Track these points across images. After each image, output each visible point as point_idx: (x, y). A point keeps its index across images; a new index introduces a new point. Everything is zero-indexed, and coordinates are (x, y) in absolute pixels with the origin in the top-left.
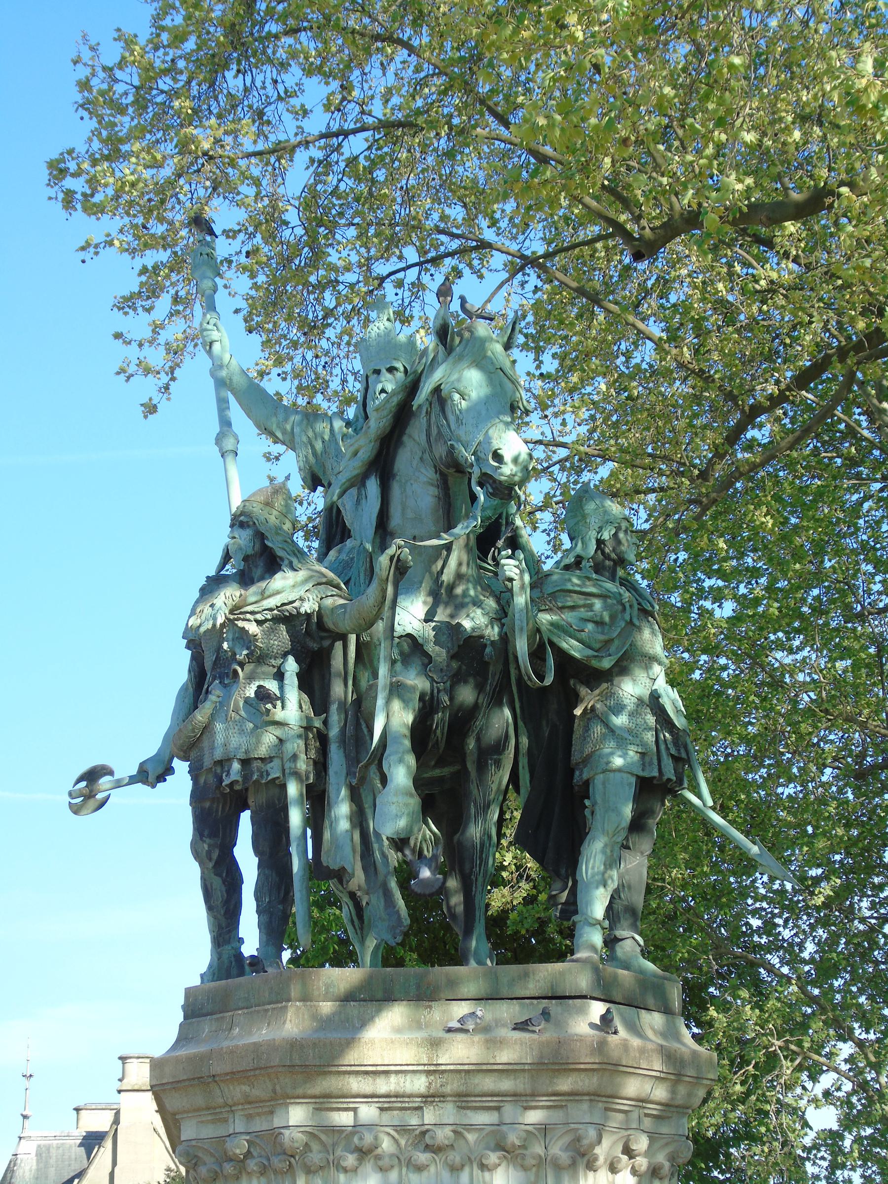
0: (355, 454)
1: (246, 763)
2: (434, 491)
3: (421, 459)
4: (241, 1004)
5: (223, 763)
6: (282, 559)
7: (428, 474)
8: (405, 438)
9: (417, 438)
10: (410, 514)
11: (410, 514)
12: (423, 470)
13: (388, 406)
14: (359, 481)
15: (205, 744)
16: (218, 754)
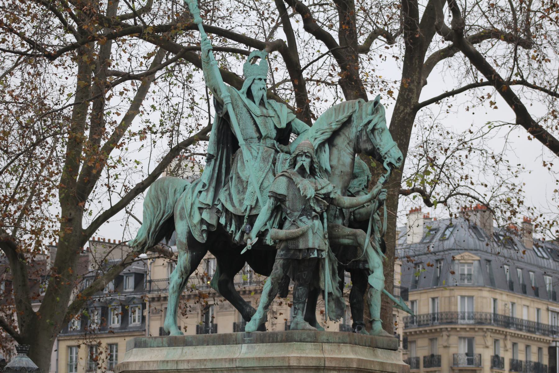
0: (322, 133)
1: (318, 250)
2: (351, 156)
3: (348, 144)
4: (324, 341)
5: (310, 250)
6: (316, 172)
7: (351, 150)
8: (341, 133)
9: (347, 135)
10: (341, 162)
11: (341, 162)
12: (349, 147)
13: (342, 121)
14: (322, 145)
15: (301, 240)
16: (310, 245)
